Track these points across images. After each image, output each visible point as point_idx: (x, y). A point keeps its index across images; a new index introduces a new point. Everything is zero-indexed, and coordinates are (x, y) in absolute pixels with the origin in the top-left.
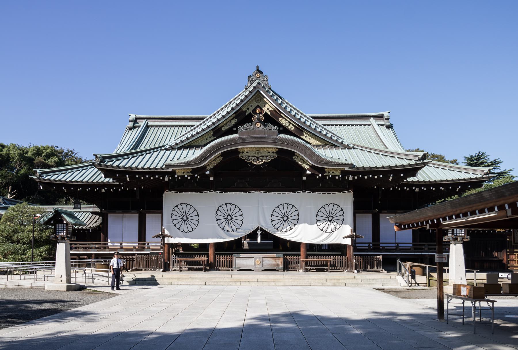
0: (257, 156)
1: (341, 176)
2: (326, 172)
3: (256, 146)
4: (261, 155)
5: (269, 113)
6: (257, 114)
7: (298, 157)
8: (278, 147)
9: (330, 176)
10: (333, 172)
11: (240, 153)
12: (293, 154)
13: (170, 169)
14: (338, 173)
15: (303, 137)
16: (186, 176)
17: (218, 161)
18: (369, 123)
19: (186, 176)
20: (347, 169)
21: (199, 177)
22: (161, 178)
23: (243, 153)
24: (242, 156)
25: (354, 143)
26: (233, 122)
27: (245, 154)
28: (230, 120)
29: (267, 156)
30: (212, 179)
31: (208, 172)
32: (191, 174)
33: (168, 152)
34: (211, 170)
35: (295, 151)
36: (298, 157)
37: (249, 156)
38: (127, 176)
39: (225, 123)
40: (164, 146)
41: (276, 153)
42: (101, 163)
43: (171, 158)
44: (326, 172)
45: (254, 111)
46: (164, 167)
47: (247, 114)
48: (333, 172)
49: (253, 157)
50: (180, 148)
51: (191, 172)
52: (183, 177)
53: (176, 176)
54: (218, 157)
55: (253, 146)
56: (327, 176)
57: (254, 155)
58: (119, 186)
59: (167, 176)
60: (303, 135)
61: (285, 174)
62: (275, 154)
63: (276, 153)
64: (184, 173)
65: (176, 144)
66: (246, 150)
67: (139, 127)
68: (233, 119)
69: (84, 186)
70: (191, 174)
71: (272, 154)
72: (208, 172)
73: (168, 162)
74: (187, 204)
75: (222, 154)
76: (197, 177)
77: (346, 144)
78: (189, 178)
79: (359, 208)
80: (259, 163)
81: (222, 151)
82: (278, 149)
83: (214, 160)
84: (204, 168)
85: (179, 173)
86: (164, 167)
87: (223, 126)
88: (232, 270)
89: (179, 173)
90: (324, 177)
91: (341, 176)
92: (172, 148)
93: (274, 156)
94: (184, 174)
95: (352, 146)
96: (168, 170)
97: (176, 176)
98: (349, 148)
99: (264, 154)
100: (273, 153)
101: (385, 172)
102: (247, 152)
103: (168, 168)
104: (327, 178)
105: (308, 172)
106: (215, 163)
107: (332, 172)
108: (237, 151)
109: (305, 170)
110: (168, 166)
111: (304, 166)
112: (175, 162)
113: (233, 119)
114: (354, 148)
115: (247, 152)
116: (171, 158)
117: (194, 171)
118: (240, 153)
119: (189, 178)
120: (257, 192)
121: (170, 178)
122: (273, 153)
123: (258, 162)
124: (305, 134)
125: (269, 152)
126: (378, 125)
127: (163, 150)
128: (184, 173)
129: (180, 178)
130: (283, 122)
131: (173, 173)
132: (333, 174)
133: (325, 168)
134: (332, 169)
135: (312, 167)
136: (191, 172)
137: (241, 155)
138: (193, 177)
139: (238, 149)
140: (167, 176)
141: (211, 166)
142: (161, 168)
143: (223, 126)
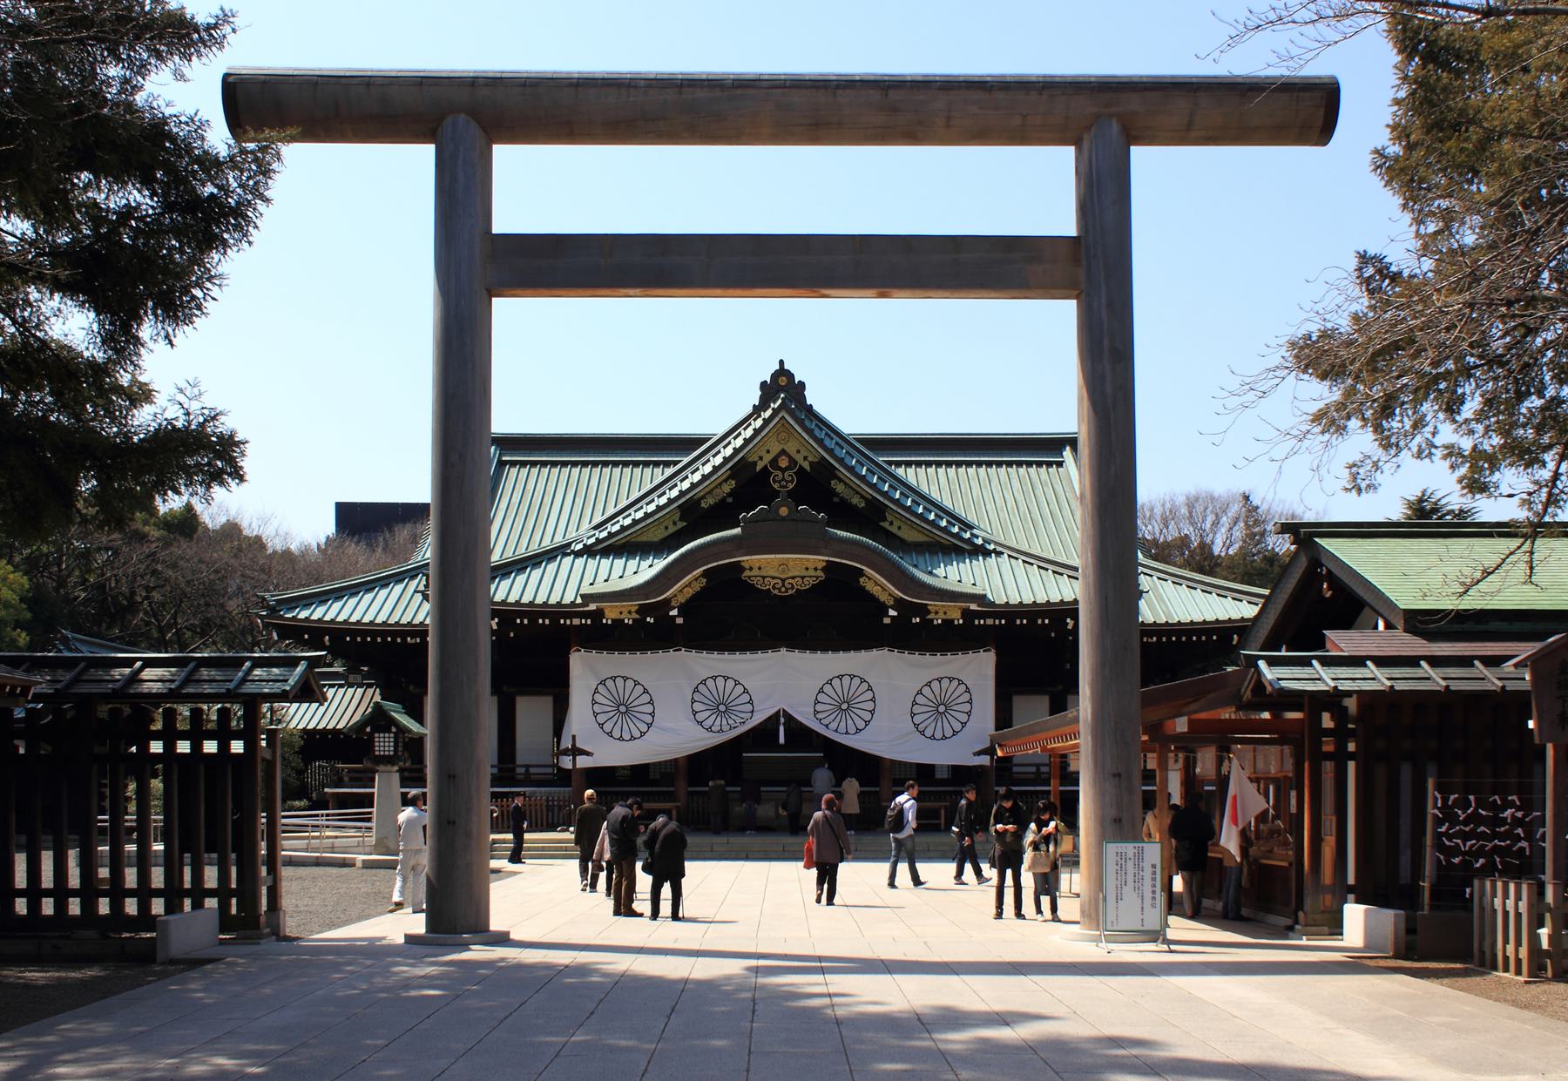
5: (806, 466)
11: (743, 569)
12: (861, 573)
13: (592, 607)
15: (886, 525)
17: (697, 587)
26: (727, 488)
27: (755, 572)
30: (680, 621)
31: (674, 612)
33: (580, 561)
40: (569, 544)
43: (588, 578)
45: (774, 462)
46: (579, 600)
47: (758, 468)
50: (605, 553)
60: (885, 519)
63: (823, 569)
65: (598, 541)
68: (725, 481)
72: (674, 612)
74: (625, 679)
75: (705, 574)
77: (979, 542)
83: (689, 585)
84: (667, 602)
85: (611, 613)
86: (579, 600)
87: (703, 497)
92: (589, 551)
95: (992, 547)
98: (987, 554)
103: (584, 604)
105: (892, 613)
106: (689, 592)
107: (944, 612)
108: (738, 568)
110: (587, 598)
111: (883, 598)
112: (600, 587)
113: (725, 481)
116: (588, 578)
117: (643, 610)
120: (783, 650)
124: (889, 518)
130: (840, 488)
131: (599, 613)
135: (899, 604)
137: (747, 573)
138: (639, 623)
141: (682, 599)
142: (573, 604)
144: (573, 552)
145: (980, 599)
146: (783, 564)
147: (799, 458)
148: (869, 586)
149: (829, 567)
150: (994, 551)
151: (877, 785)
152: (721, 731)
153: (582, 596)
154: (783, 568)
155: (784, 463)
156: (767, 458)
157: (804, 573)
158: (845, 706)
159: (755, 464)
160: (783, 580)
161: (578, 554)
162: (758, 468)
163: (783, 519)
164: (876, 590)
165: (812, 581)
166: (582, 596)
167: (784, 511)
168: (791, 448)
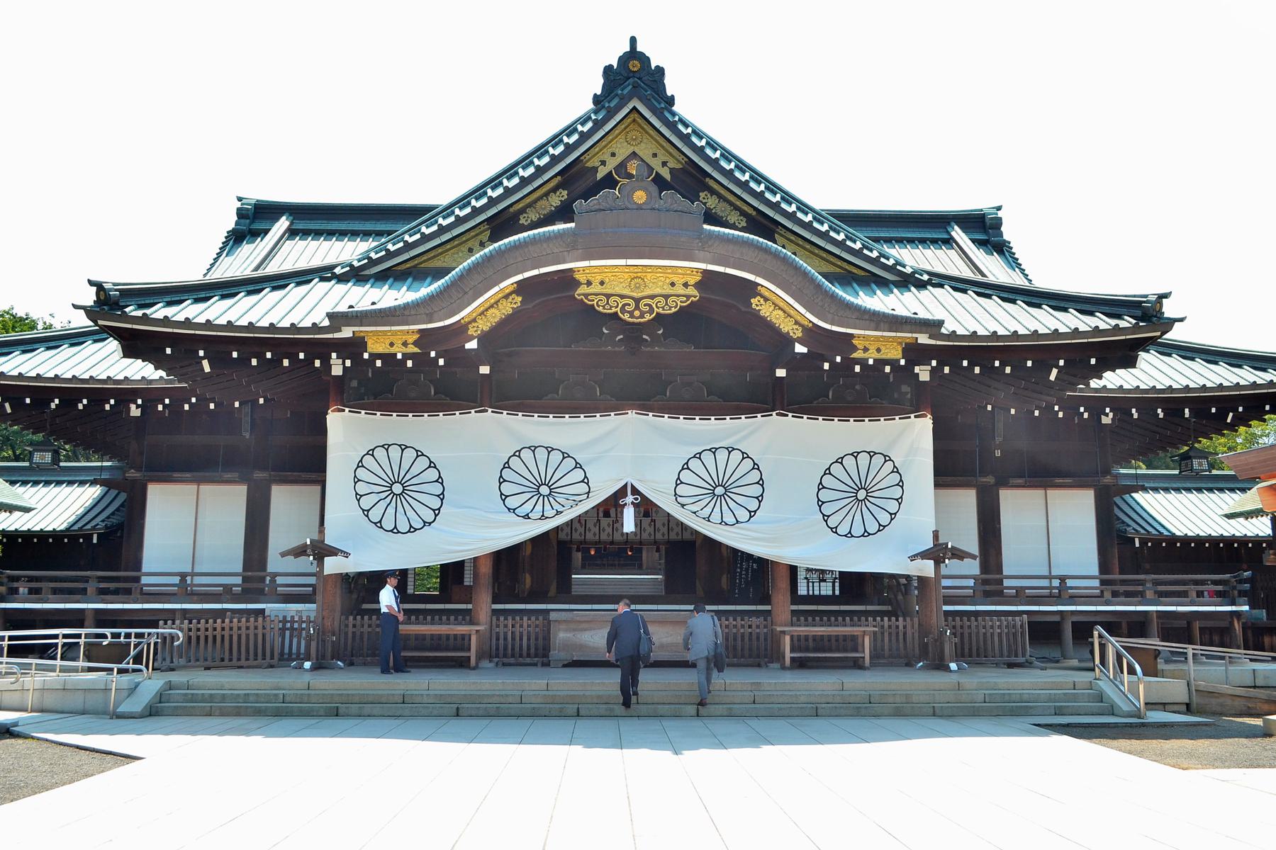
0: (634, 294)
1: (903, 362)
2: (855, 349)
3: (630, 262)
4: (648, 292)
6: (630, 176)
7: (766, 299)
8: (703, 266)
9: (871, 362)
10: (879, 350)
11: (577, 284)
12: (752, 288)
13: (347, 333)
14: (895, 353)
16: (399, 356)
17: (507, 308)
18: (946, 236)
19: (399, 356)
20: (923, 339)
21: (441, 362)
22: (317, 363)
23: (589, 283)
24: (586, 295)
25: (929, 268)
27: (596, 288)
28: (546, 194)
29: (666, 297)
32: (417, 350)
33: (341, 288)
34: (483, 338)
35: (759, 280)
36: (766, 299)
37: (608, 296)
38: (201, 353)
39: (528, 200)
40: (332, 267)
41: (697, 286)
42: (112, 310)
44: (855, 349)
45: (622, 166)
46: (326, 323)
48: (879, 350)
49: (622, 297)
51: (415, 343)
52: (388, 358)
53: (366, 356)
54: (506, 297)
55: (622, 262)
56: (857, 361)
57: (626, 292)
58: (179, 397)
59: (334, 355)
61: (719, 362)
62: (692, 291)
63: (697, 286)
64: (392, 344)
66: (599, 278)
67: (266, 232)
68: (554, 190)
69: (70, 392)
70: (417, 350)
71: (682, 291)
72: (472, 345)
73: (343, 308)
75: (521, 287)
76: (436, 359)
77: (908, 270)
78: (410, 364)
79: (948, 471)
80: (642, 316)
81: (519, 277)
82: (705, 272)
84: (460, 330)
85: (378, 342)
86: (326, 323)
87: (523, 211)
88: (544, 665)
89: (376, 346)
90: (849, 363)
91: (903, 362)
93: (688, 297)
94: (392, 350)
95: (926, 277)
96: (337, 335)
97: (366, 356)
98: (921, 285)
99: (658, 291)
100: (686, 285)
101: (1042, 351)
102: (602, 283)
104: (857, 369)
105: (800, 349)
106: (495, 316)
108: (567, 281)
109: (788, 341)
110: (337, 319)
111: (787, 326)
113: (554, 190)
114: (935, 286)
115: (602, 283)
117: (426, 338)
118: (577, 284)
119: (410, 364)
121: (348, 363)
122: (686, 285)
123: (637, 313)
125: (673, 284)
126: (973, 241)
127: (328, 279)
128: (392, 344)
129: (379, 363)
132: (878, 356)
133: (852, 336)
134: (877, 339)
135: (812, 334)
136: (415, 343)
137: (583, 289)
139: (571, 270)
140: (334, 355)
141: (484, 325)
142: (315, 328)
143: (523, 211)
144: (334, 276)
145: (933, 326)
146: (637, 276)
147: (656, 164)
148: (766, 311)
149: (708, 281)
150: (929, 283)
151: (769, 604)
152: (543, 517)
153: (331, 316)
154: (640, 279)
155: (633, 168)
156: (612, 164)
157: (669, 291)
158: (720, 490)
159: (595, 170)
160: (637, 301)
161: (342, 279)
162: (600, 176)
163: (640, 208)
164: (776, 317)
165: (681, 303)
166: (331, 316)
167: (640, 197)
168: (645, 150)
